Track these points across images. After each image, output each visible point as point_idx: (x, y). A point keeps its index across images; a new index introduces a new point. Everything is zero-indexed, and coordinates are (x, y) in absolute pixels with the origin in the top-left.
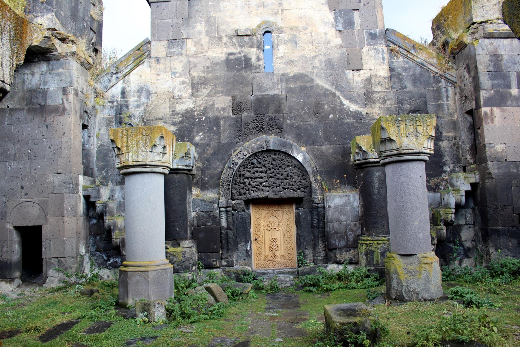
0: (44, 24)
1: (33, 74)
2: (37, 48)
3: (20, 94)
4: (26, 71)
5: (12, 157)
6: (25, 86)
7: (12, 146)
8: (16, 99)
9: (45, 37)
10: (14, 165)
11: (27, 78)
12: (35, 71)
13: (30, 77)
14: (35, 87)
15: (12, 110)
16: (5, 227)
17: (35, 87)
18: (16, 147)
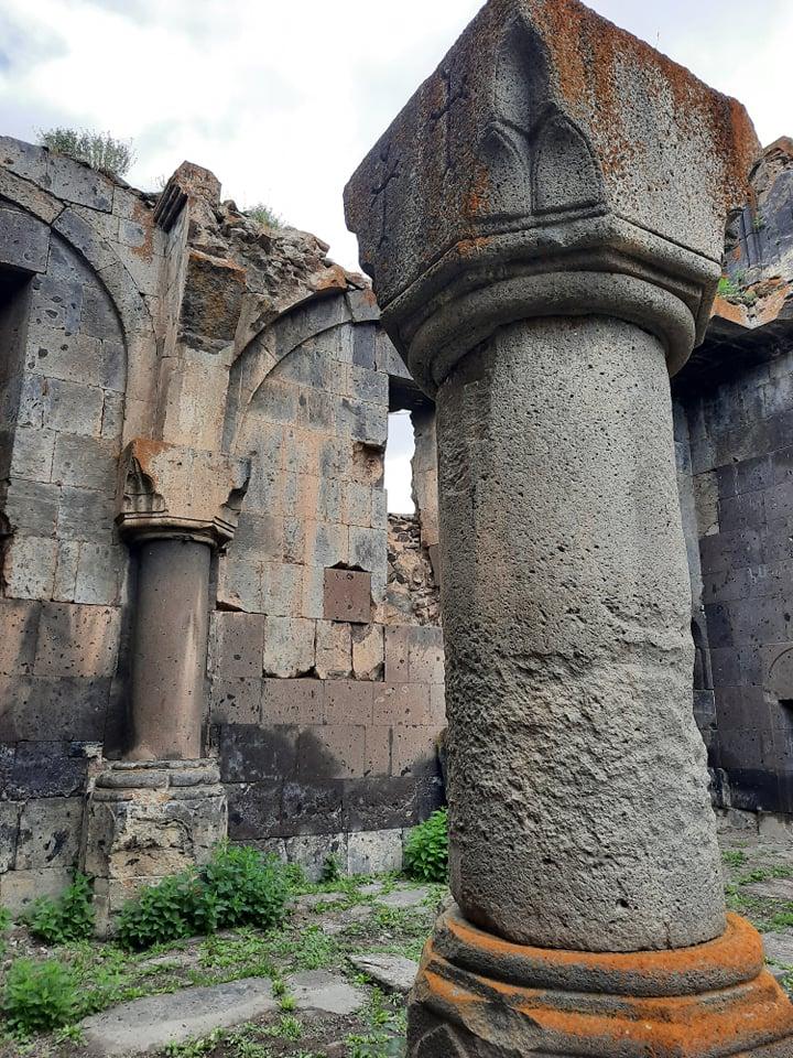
0: (783, 275)
1: (775, 383)
2: (775, 326)
3: (755, 431)
4: (761, 382)
5: (757, 557)
6: (763, 411)
7: (754, 534)
8: (748, 441)
9: (788, 298)
10: (763, 572)
11: (765, 394)
12: (779, 376)
13: (769, 391)
14: (783, 407)
15: (742, 465)
16: (763, 699)
17: (783, 407)
18: (763, 535)
